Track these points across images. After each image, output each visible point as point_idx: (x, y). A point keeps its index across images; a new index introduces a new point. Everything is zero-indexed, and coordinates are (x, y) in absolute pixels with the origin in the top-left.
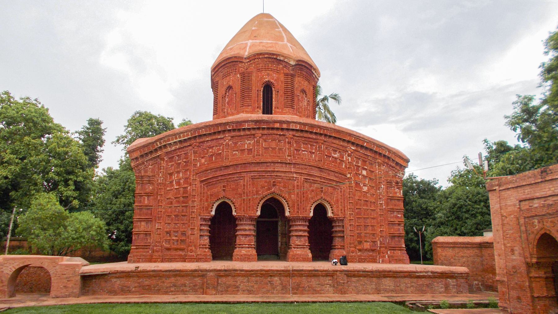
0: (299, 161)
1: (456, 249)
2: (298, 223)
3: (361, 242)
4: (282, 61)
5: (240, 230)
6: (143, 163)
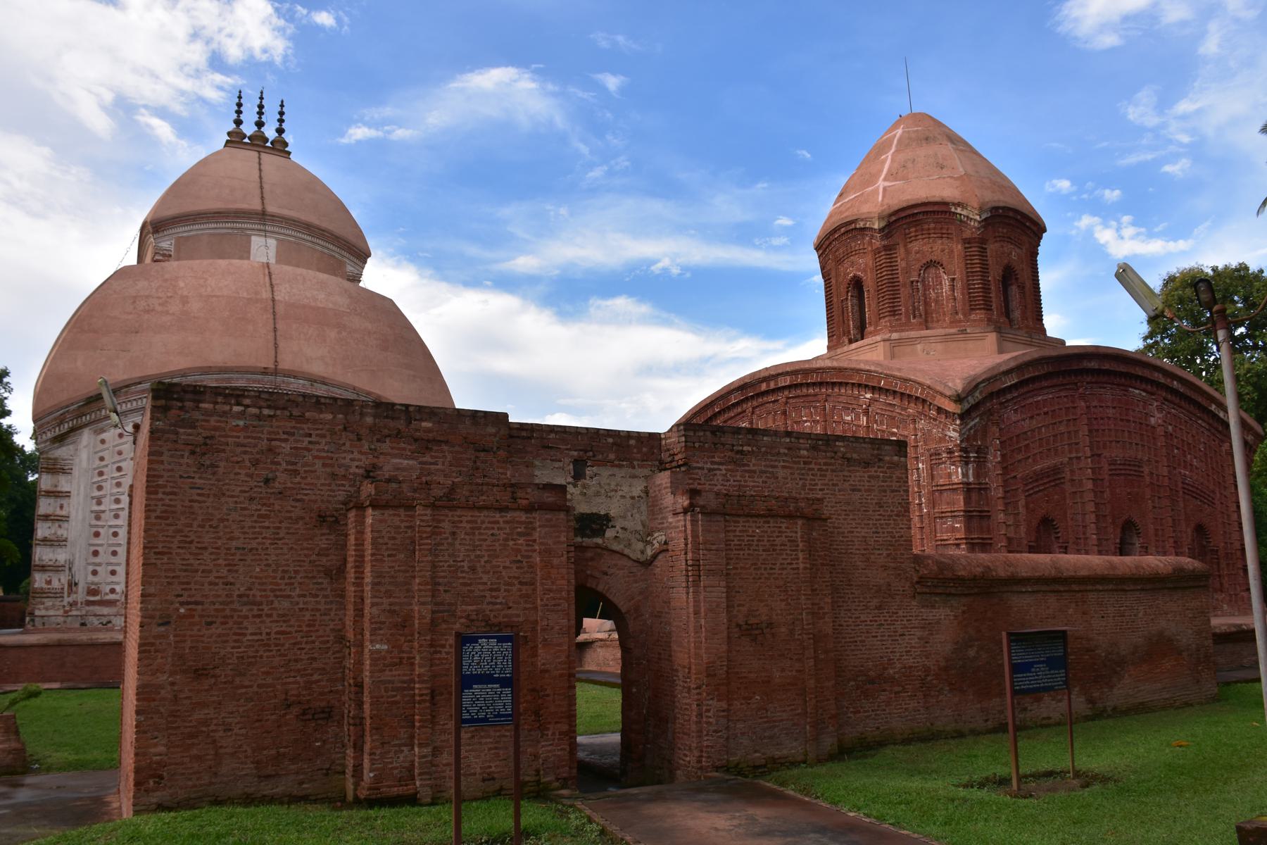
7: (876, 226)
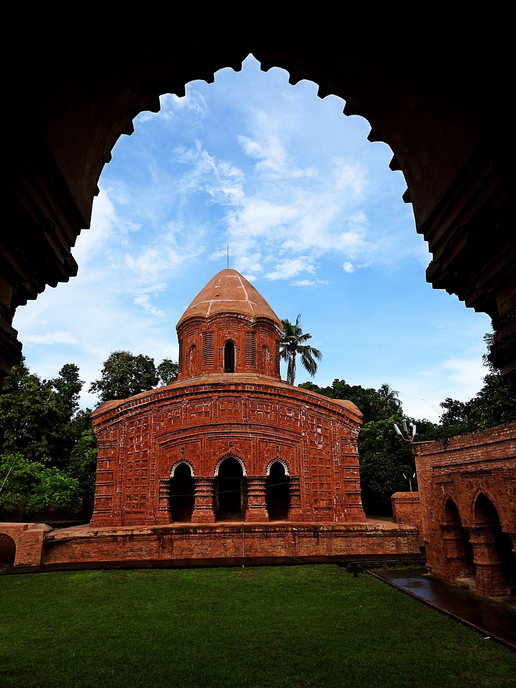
0: (254, 422)
1: (414, 504)
2: (255, 483)
3: (317, 500)
4: (243, 319)
5: (198, 491)
6: (105, 429)
7: (252, 321)
